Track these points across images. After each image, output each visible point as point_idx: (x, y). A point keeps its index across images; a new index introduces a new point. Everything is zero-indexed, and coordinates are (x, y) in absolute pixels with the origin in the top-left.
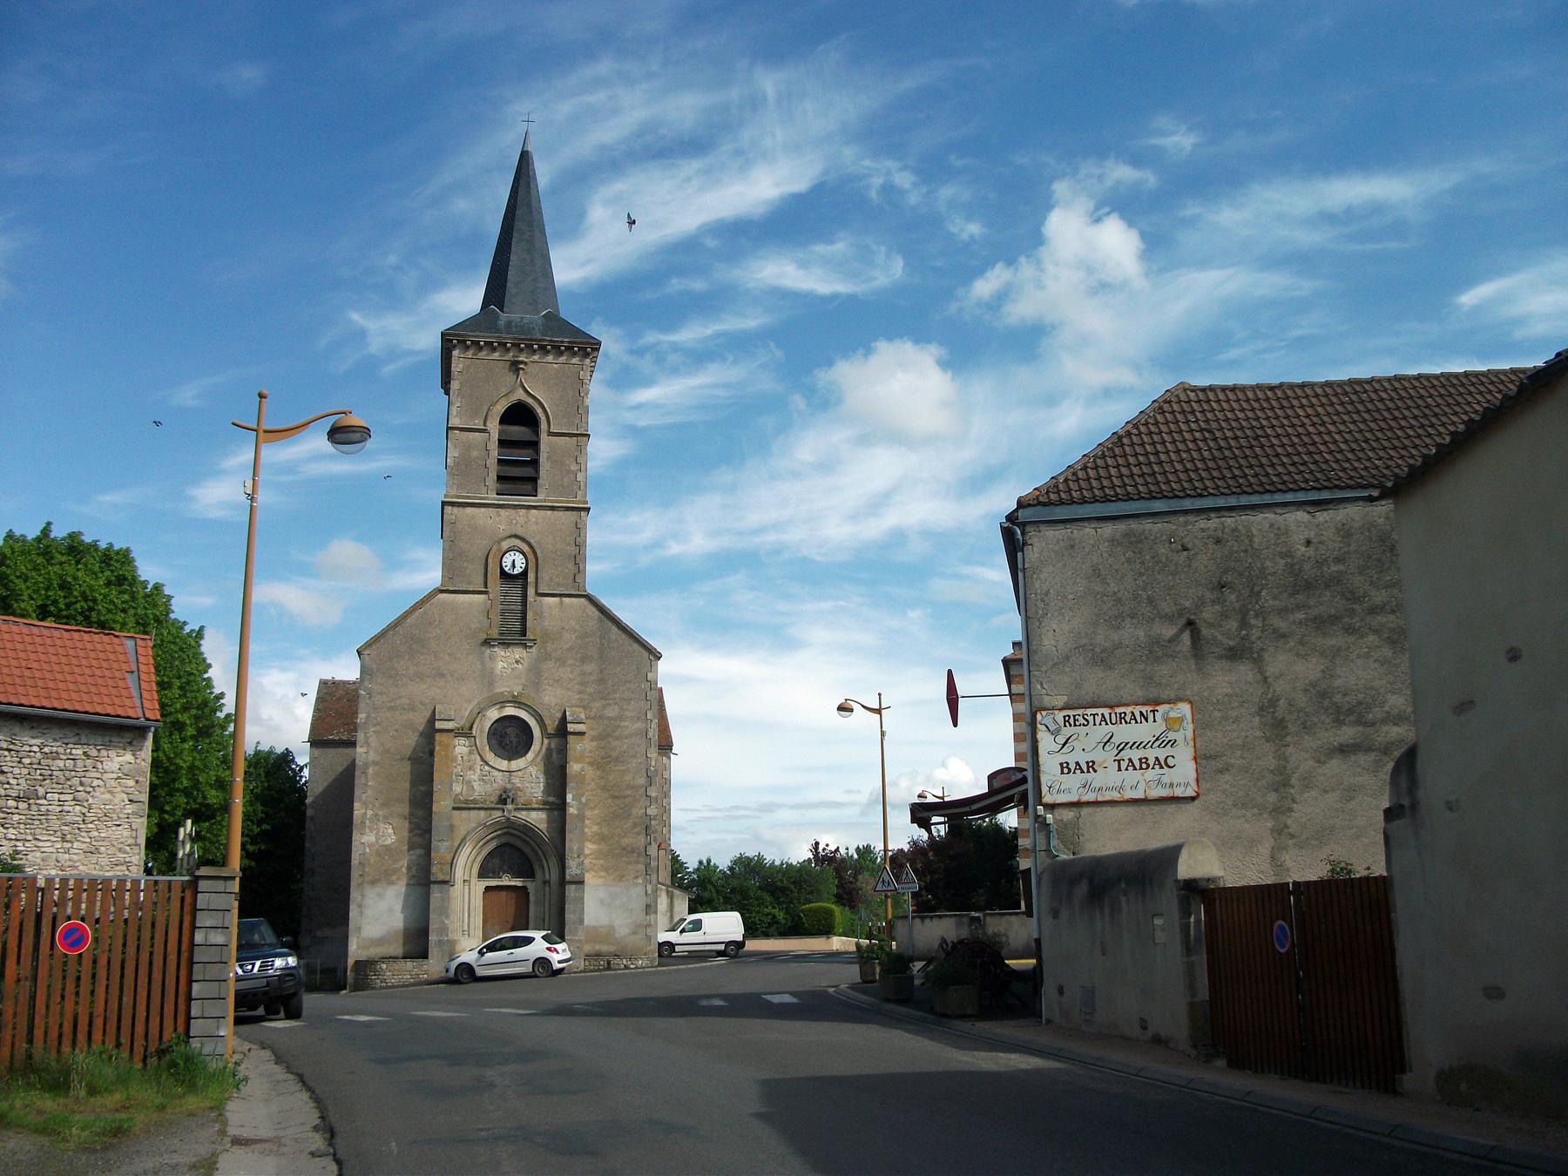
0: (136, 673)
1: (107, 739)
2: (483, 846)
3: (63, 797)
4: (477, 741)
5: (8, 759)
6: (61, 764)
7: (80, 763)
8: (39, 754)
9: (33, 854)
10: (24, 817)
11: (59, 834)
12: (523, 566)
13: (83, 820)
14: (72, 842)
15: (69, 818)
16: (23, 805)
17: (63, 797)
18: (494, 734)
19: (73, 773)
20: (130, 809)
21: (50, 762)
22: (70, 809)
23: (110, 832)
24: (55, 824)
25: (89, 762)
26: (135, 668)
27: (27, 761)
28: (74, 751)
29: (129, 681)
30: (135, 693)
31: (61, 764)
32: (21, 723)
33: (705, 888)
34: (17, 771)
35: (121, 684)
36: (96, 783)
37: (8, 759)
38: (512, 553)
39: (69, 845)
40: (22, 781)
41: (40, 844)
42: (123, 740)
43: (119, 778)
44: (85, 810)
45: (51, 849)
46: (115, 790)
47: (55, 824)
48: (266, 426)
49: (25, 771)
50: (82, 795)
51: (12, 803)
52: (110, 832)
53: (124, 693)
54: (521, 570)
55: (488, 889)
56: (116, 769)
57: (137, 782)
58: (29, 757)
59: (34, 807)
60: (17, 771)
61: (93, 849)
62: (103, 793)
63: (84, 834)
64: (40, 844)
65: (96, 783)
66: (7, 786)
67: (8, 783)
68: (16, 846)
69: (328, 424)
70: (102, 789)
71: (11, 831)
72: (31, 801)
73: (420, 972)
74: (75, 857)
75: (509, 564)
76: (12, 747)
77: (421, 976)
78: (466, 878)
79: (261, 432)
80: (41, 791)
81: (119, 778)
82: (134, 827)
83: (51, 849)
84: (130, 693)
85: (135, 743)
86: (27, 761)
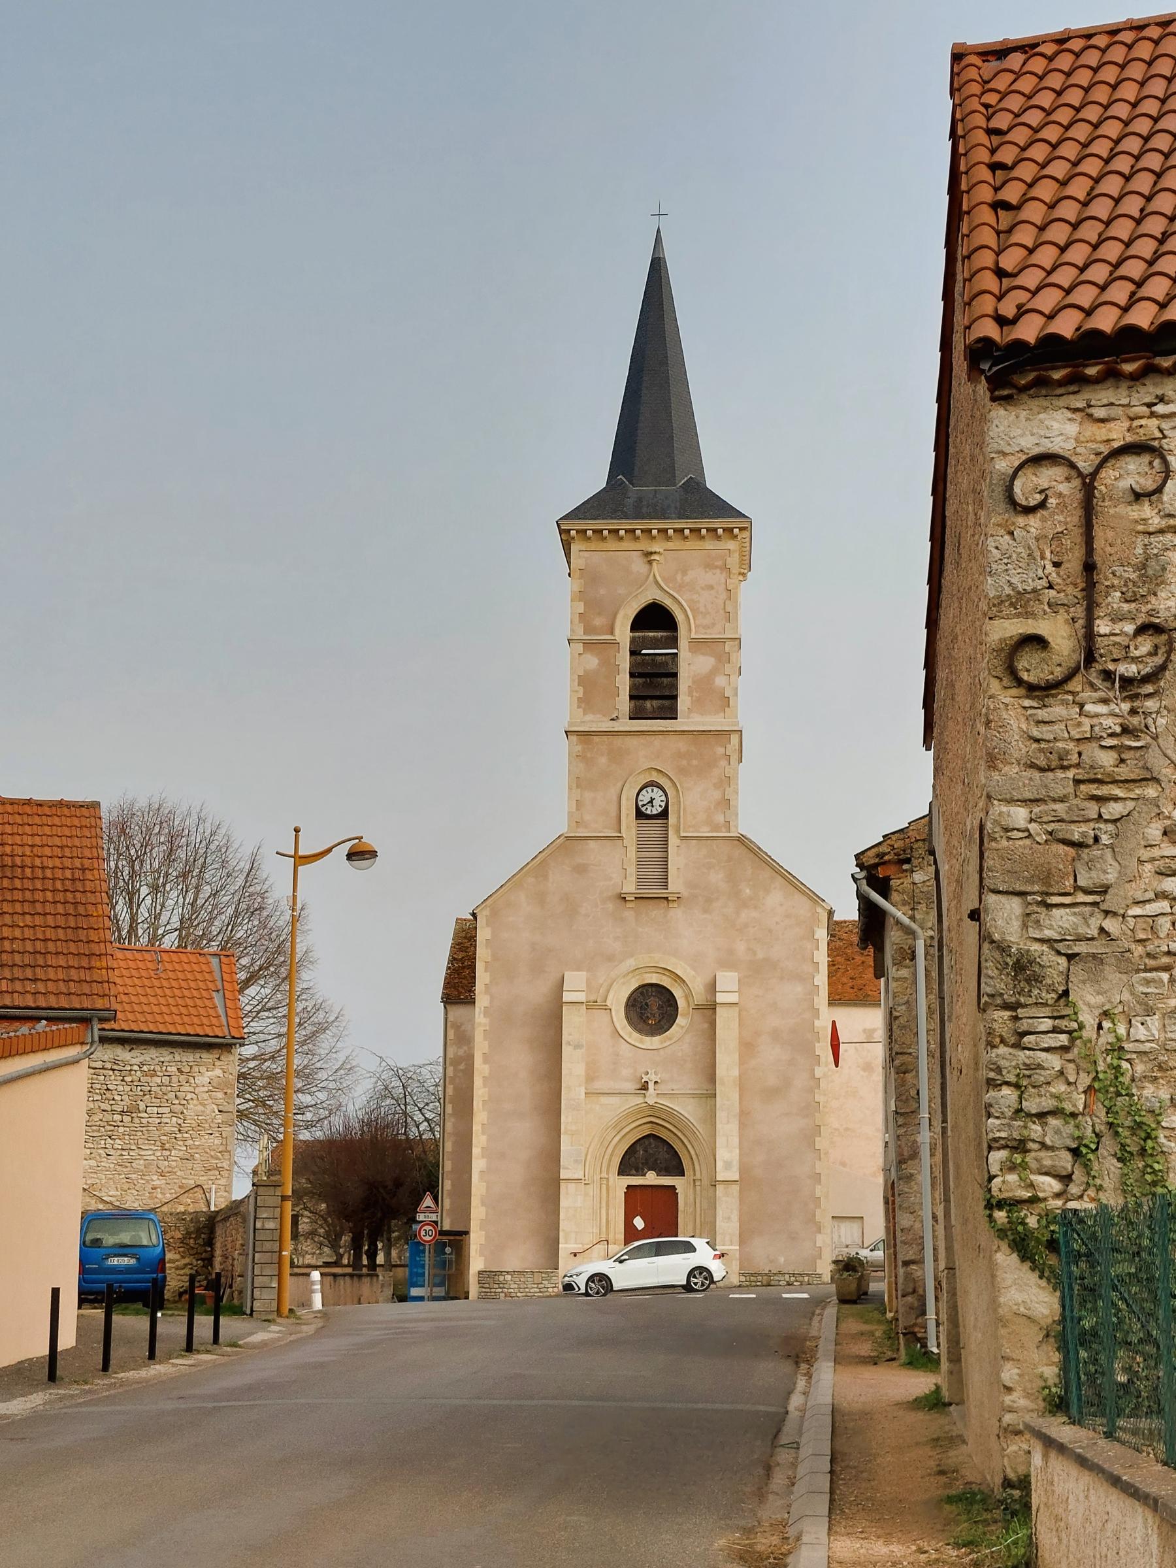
0: (221, 992)
1: (198, 1055)
2: (620, 1140)
3: (161, 1110)
4: (613, 1013)
5: (113, 1077)
6: (158, 1080)
7: (174, 1079)
8: (139, 1073)
9: (137, 1162)
10: (128, 1129)
11: (158, 1143)
12: (663, 804)
13: (179, 1130)
14: (170, 1151)
15: (167, 1129)
16: (127, 1119)
17: (161, 1110)
18: (633, 1006)
19: (169, 1088)
20: (219, 1119)
21: (148, 1079)
22: (168, 1120)
23: (203, 1140)
24: (155, 1134)
25: (182, 1078)
26: (220, 987)
27: (128, 1079)
28: (169, 1068)
29: (216, 1000)
30: (223, 1019)
31: (158, 1080)
32: (123, 1045)
33: (1157, 1175)
34: (120, 1088)
35: (208, 1003)
36: (189, 1096)
37: (113, 1077)
38: (649, 789)
39: (168, 1153)
40: (125, 1097)
41: (143, 1153)
42: (211, 1056)
43: (210, 1091)
44: (180, 1121)
45: (152, 1157)
46: (206, 1102)
47: (155, 1134)
48: (300, 853)
49: (128, 1088)
50: (177, 1108)
51: (117, 1117)
52: (203, 1140)
53: (212, 1012)
54: (660, 809)
55: (629, 1187)
56: (206, 1083)
57: (226, 1093)
58: (130, 1075)
59: (136, 1120)
60: (120, 1088)
61: (188, 1156)
62: (195, 1105)
63: (181, 1143)
64: (143, 1153)
65: (189, 1096)
66: (113, 1102)
67: (113, 1099)
68: (122, 1155)
69: (346, 848)
70: (195, 1102)
71: (118, 1141)
72: (133, 1115)
73: (549, 1285)
74: (174, 1164)
75: (647, 800)
76: (115, 1067)
77: (550, 1290)
78: (604, 1175)
79: (297, 859)
80: (142, 1106)
81: (210, 1091)
82: (224, 1136)
83: (152, 1157)
84: (214, 1004)
85: (222, 1058)
86: (128, 1079)
